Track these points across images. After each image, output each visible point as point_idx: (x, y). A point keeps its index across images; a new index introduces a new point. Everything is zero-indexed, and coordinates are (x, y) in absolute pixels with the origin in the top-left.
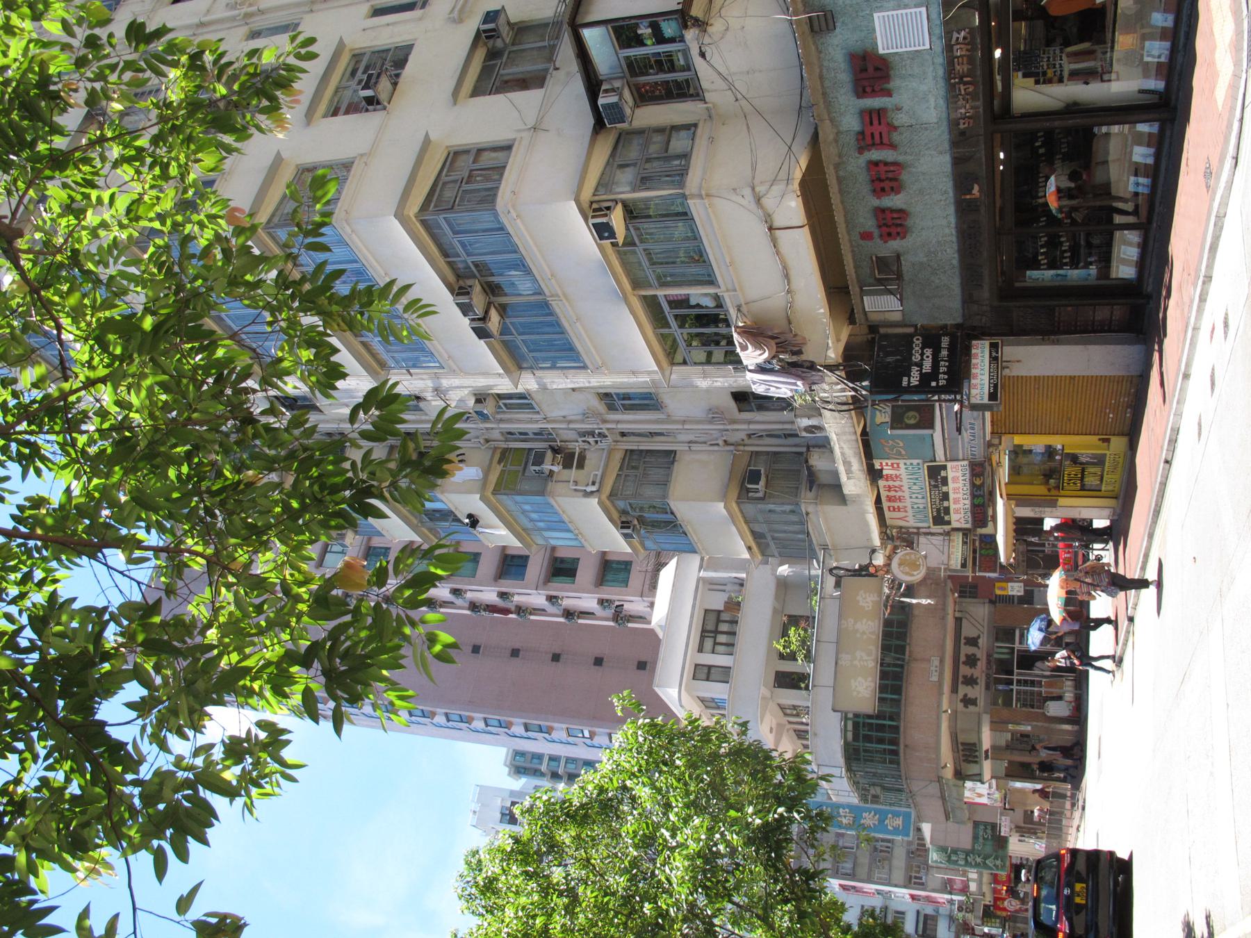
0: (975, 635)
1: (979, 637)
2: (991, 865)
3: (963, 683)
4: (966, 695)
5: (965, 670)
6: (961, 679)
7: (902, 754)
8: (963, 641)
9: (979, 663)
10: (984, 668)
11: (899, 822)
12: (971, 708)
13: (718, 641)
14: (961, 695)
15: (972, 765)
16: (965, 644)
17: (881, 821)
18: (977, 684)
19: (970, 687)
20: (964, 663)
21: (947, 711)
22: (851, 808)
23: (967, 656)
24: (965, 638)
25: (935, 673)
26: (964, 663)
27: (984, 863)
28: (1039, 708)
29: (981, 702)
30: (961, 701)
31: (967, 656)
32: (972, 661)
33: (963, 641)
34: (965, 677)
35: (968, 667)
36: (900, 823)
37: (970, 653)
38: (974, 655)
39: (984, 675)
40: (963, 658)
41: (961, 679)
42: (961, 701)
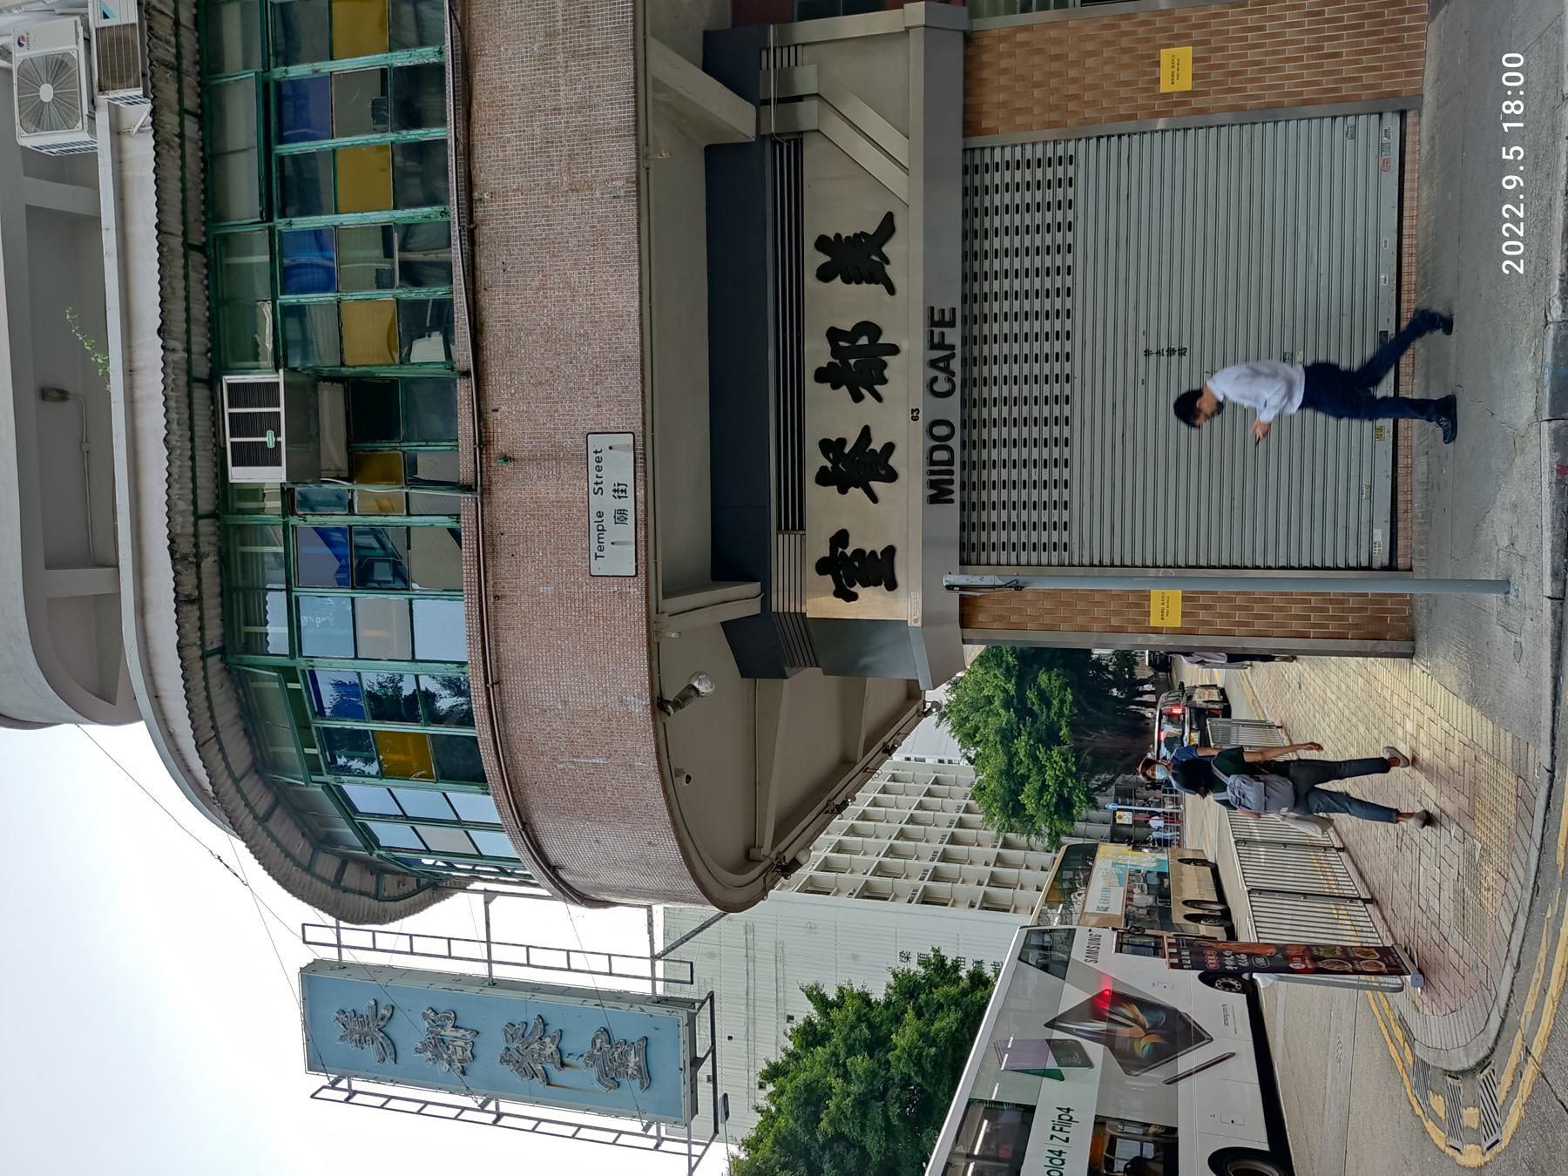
1: (887, 227)
3: (823, 478)
4: (841, 538)
6: (815, 460)
8: (814, 259)
10: (918, 397)
16: (825, 274)
18: (892, 476)
19: (856, 493)
20: (821, 375)
23: (834, 335)
24: (822, 243)
26: (821, 375)
30: (823, 567)
33: (814, 259)
37: (847, 326)
40: (817, 352)
41: (815, 460)
42: (823, 567)
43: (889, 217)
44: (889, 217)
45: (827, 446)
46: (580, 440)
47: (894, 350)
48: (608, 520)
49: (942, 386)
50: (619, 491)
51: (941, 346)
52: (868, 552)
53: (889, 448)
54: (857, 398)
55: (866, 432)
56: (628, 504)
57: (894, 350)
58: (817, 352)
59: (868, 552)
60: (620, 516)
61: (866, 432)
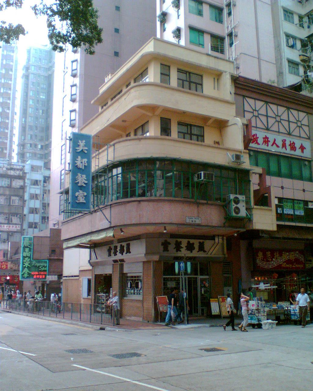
0: (205, 249)
1: (204, 251)
2: (24, 271)
3: (177, 241)
4: (169, 244)
5: (184, 243)
7: (133, 199)
8: (201, 241)
9: (189, 252)
10: (187, 255)
11: (82, 200)
12: (162, 248)
13: (185, 82)
14: (169, 240)
15: (107, 253)
16: (200, 243)
17: (81, 187)
19: (174, 246)
20: (189, 242)
21: (165, 229)
22: (88, 167)
23: (193, 244)
24: (203, 242)
25: (191, 220)
26: (189, 242)
27: (25, 267)
28: (164, 293)
29: (166, 254)
30: (166, 241)
31: (193, 244)
32: (190, 247)
34: (181, 242)
35: (186, 245)
36: (81, 201)
38: (194, 248)
39: (183, 255)
40: (192, 241)
41: (179, 240)
42: (166, 241)
43: (206, 252)
44: (206, 252)
45: (181, 242)
46: (200, 216)
47: (191, 252)
48: (192, 219)
49: (187, 258)
50: (195, 221)
51: (192, 259)
52: (163, 246)
53: (180, 251)
54: (186, 247)
55: (182, 248)
56: (194, 222)
57: (191, 252)
58: (192, 241)
59: (163, 246)
60: (192, 221)
61: (182, 248)
